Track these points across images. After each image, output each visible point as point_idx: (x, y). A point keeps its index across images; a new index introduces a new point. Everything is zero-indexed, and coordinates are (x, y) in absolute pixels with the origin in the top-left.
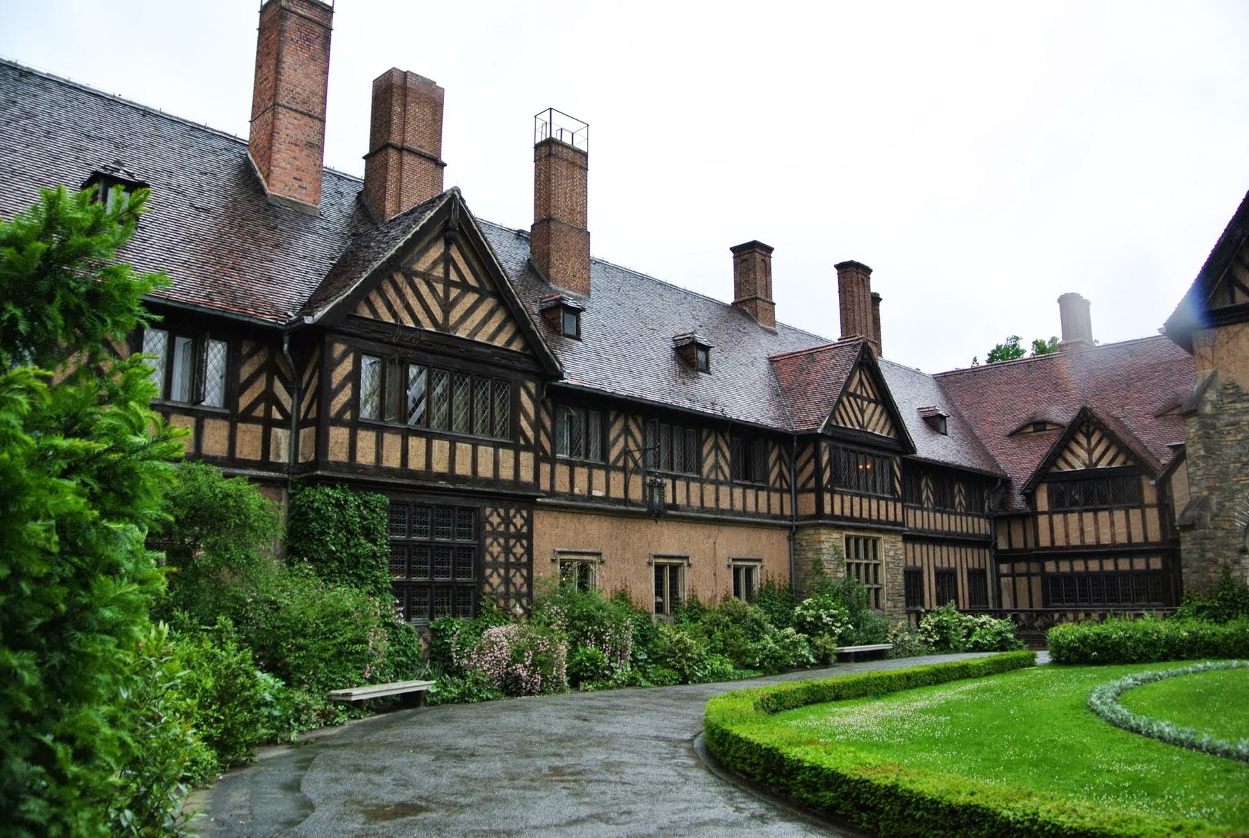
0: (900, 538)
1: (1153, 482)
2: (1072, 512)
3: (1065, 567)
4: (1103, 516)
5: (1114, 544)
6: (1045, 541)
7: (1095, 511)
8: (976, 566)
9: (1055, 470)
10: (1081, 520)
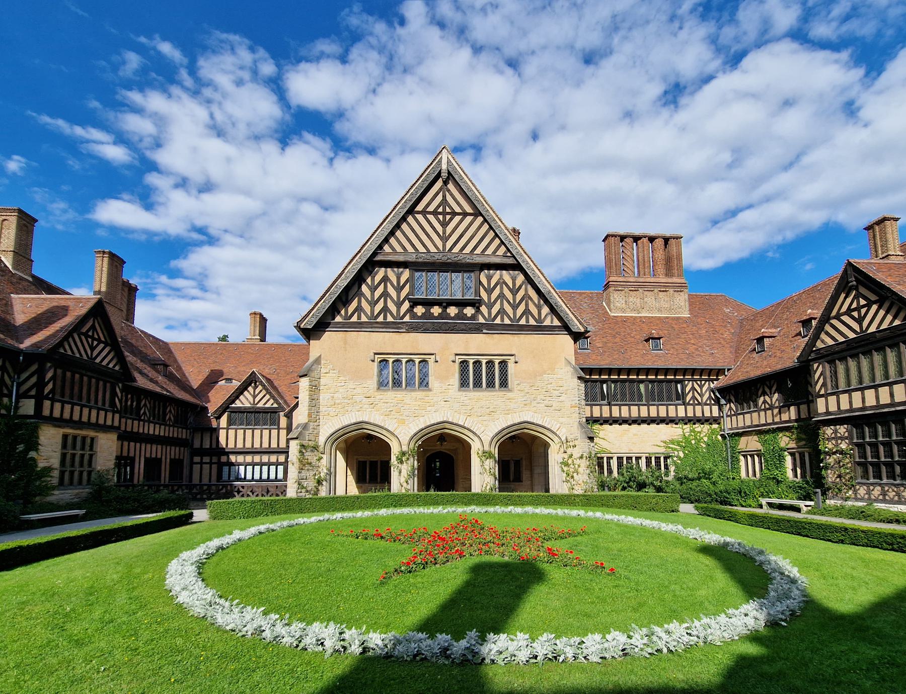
0: (114, 436)
8: (177, 457)
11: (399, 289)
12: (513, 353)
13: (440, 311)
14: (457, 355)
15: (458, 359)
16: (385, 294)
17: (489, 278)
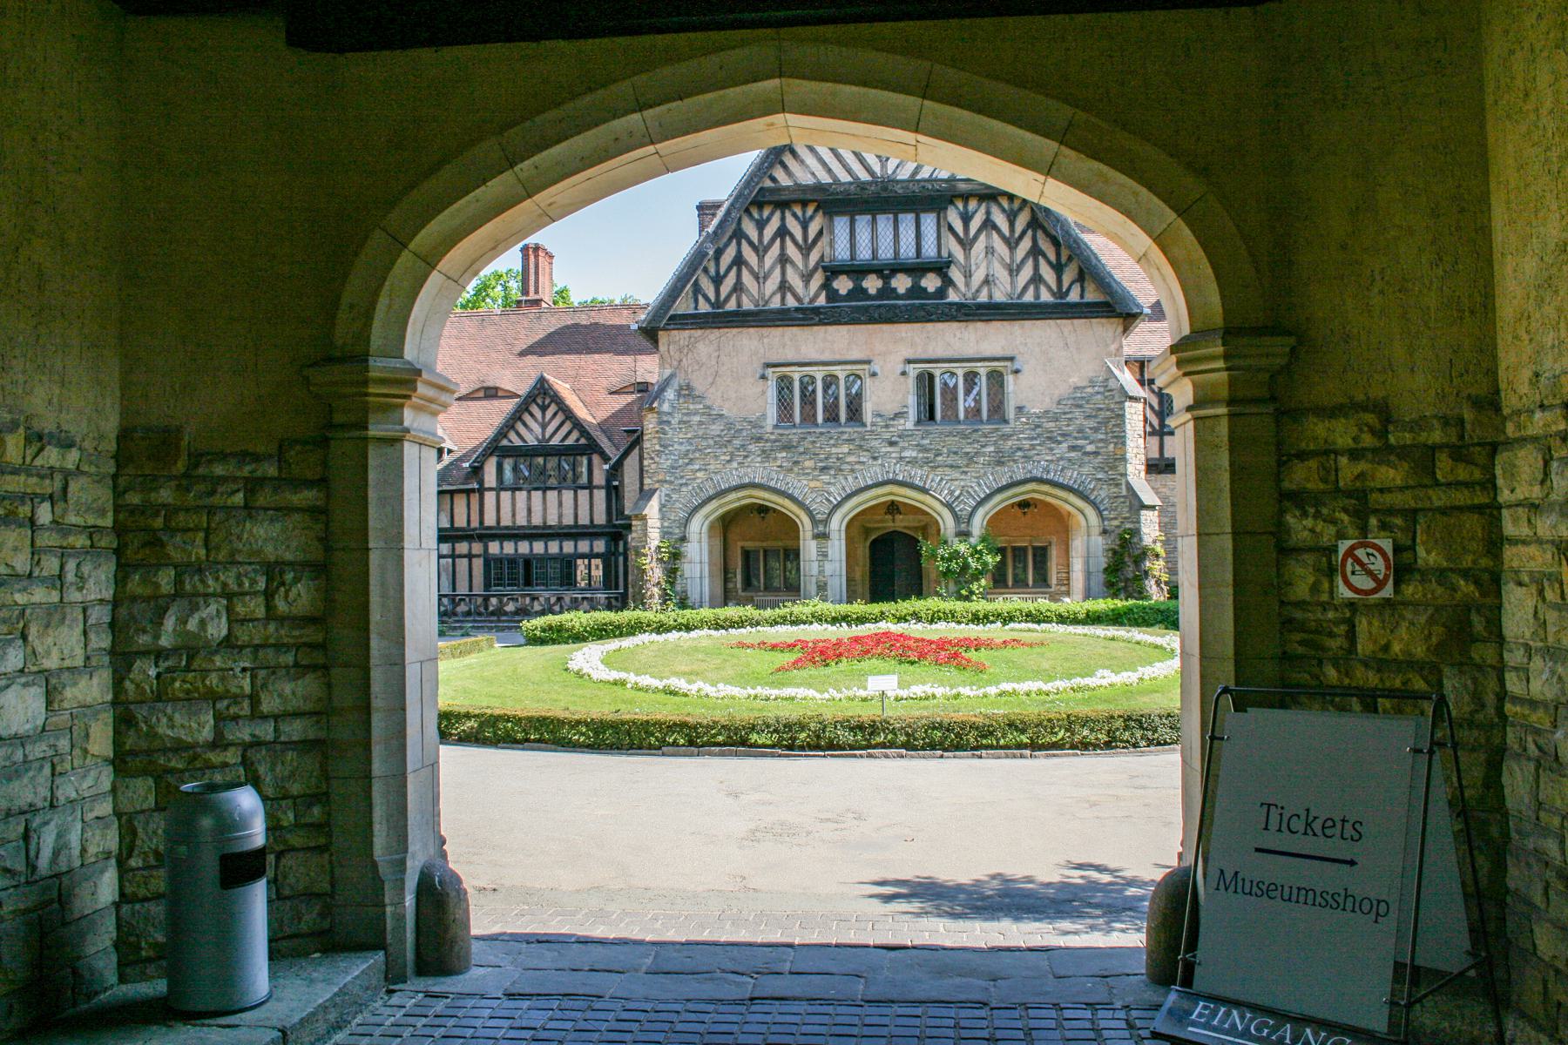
1: (606, 467)
2: (520, 489)
3: (509, 548)
4: (552, 495)
5: (560, 526)
6: (490, 520)
7: (545, 490)
9: (505, 442)
10: (529, 498)
11: (806, 249)
12: (1008, 354)
13: (879, 283)
14: (909, 362)
15: (913, 370)
16: (784, 260)
17: (966, 219)
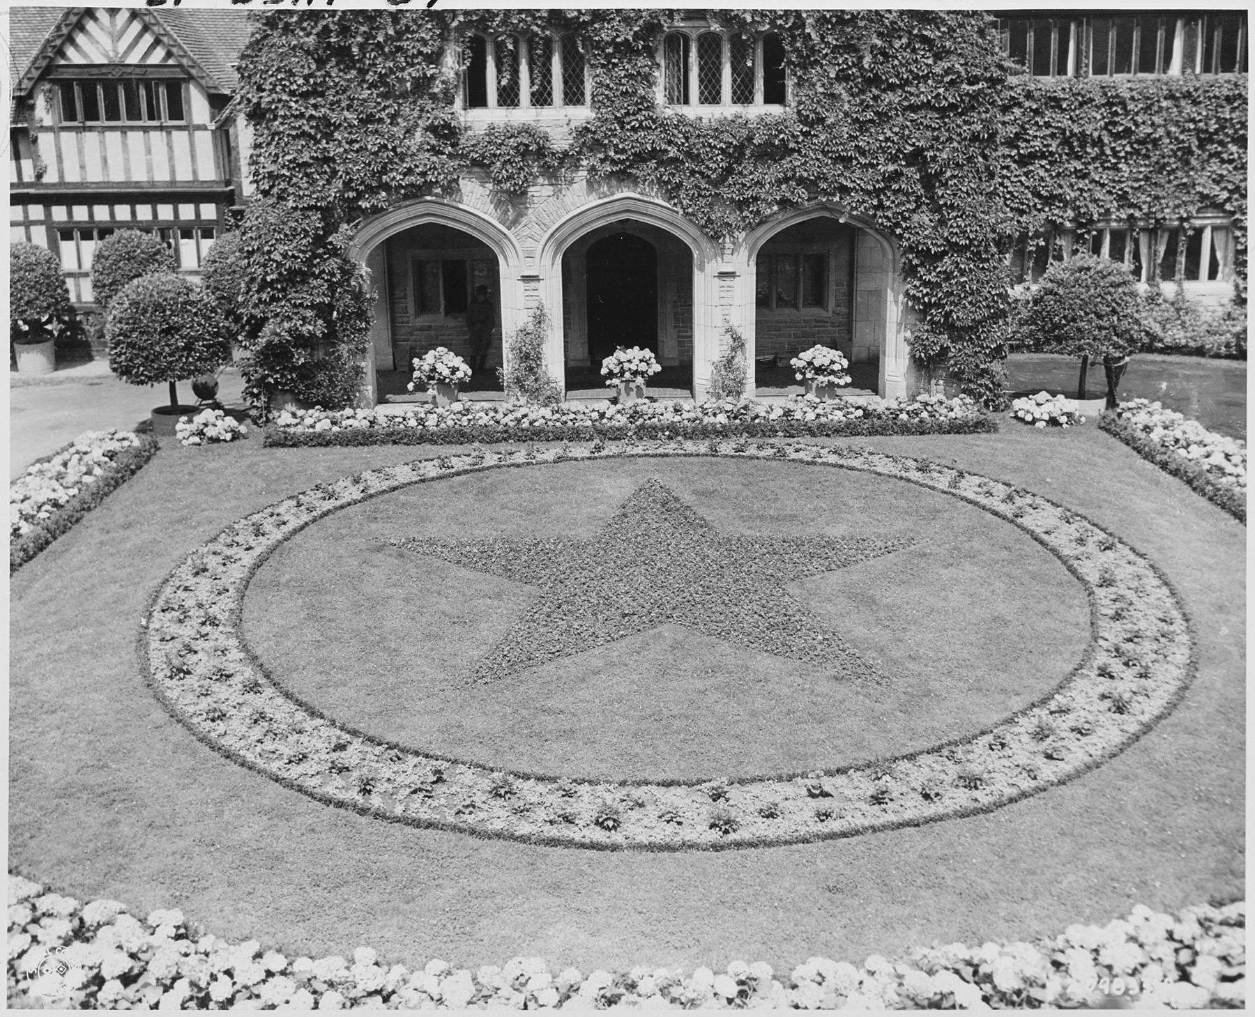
2: (91, 129)
9: (63, 62)
